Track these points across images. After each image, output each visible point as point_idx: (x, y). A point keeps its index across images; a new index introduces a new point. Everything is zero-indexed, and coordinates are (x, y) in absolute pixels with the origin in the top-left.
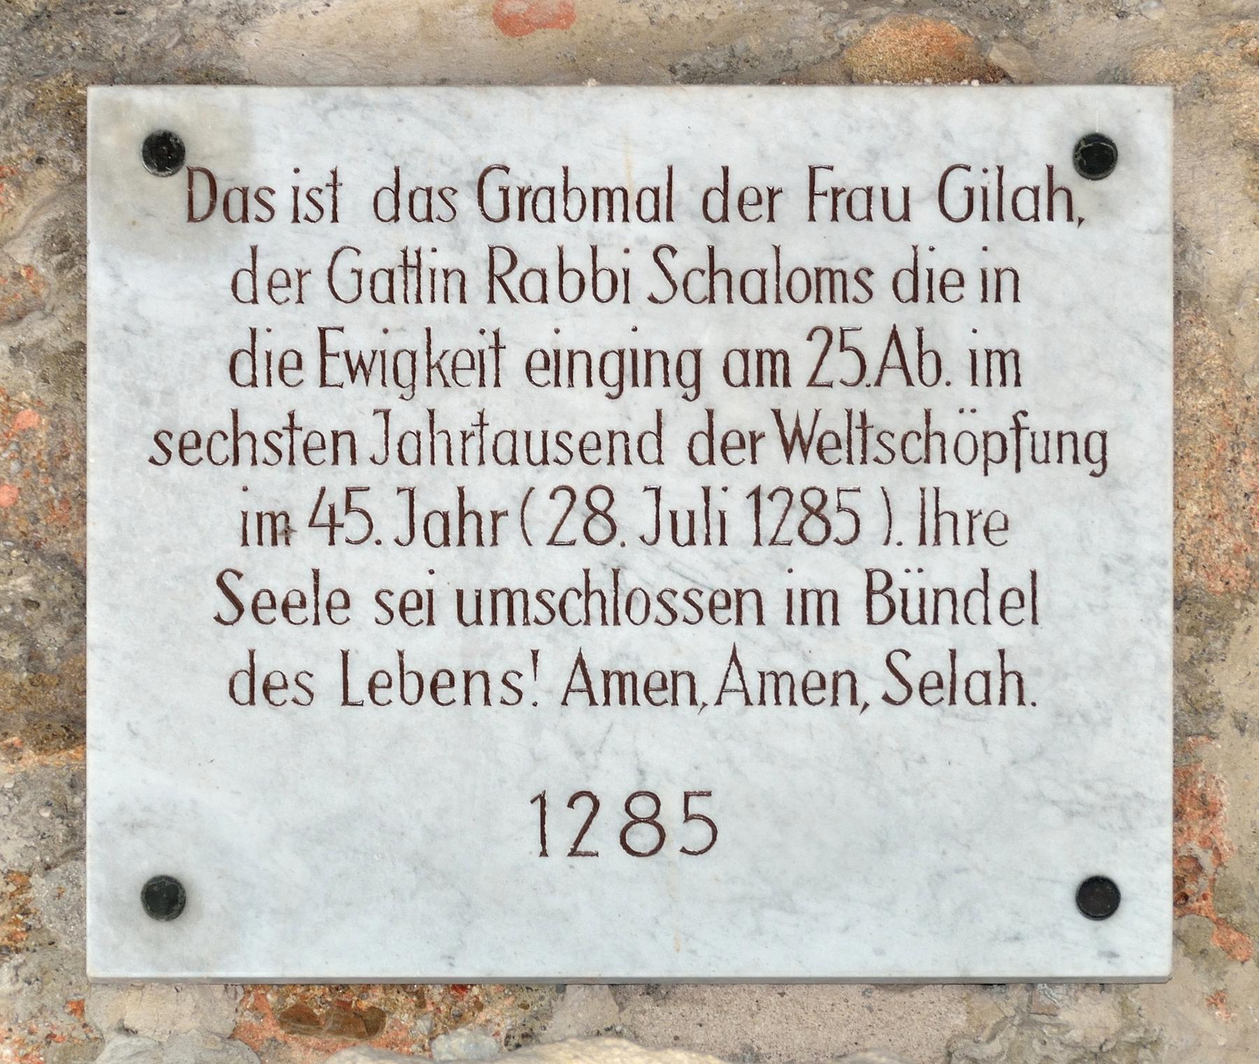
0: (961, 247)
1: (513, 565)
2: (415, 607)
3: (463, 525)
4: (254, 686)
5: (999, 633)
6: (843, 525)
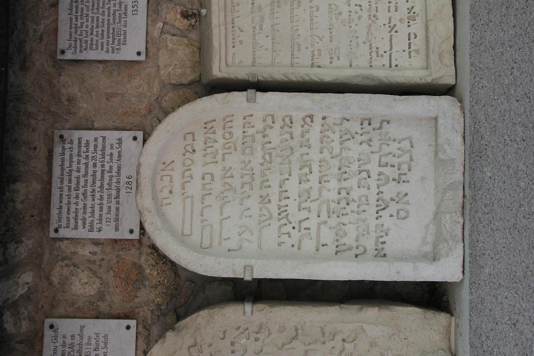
0: (60, 340)
5: (100, 337)
6: (89, 353)
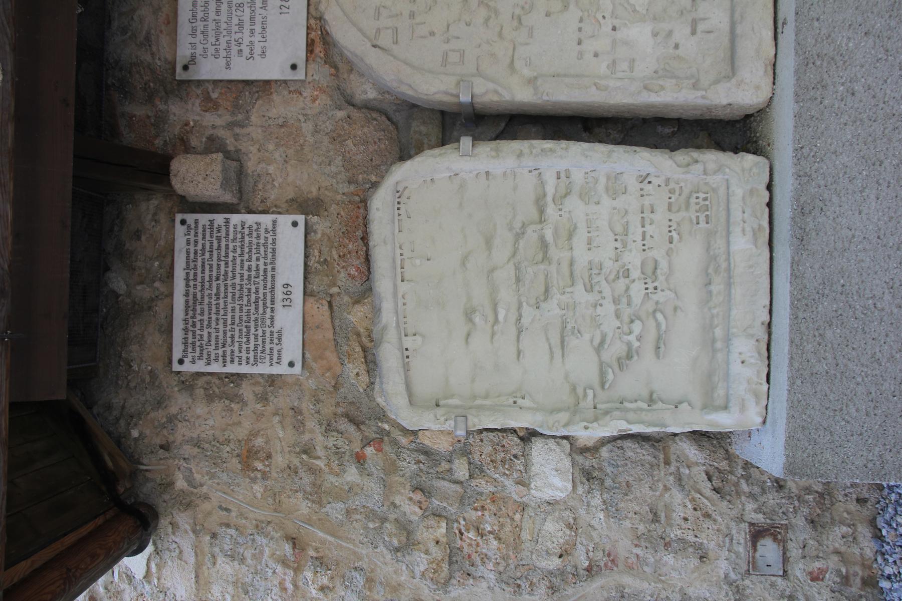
1: (246, 17)
2: (252, 32)
3: (240, 25)
4: (263, 54)
